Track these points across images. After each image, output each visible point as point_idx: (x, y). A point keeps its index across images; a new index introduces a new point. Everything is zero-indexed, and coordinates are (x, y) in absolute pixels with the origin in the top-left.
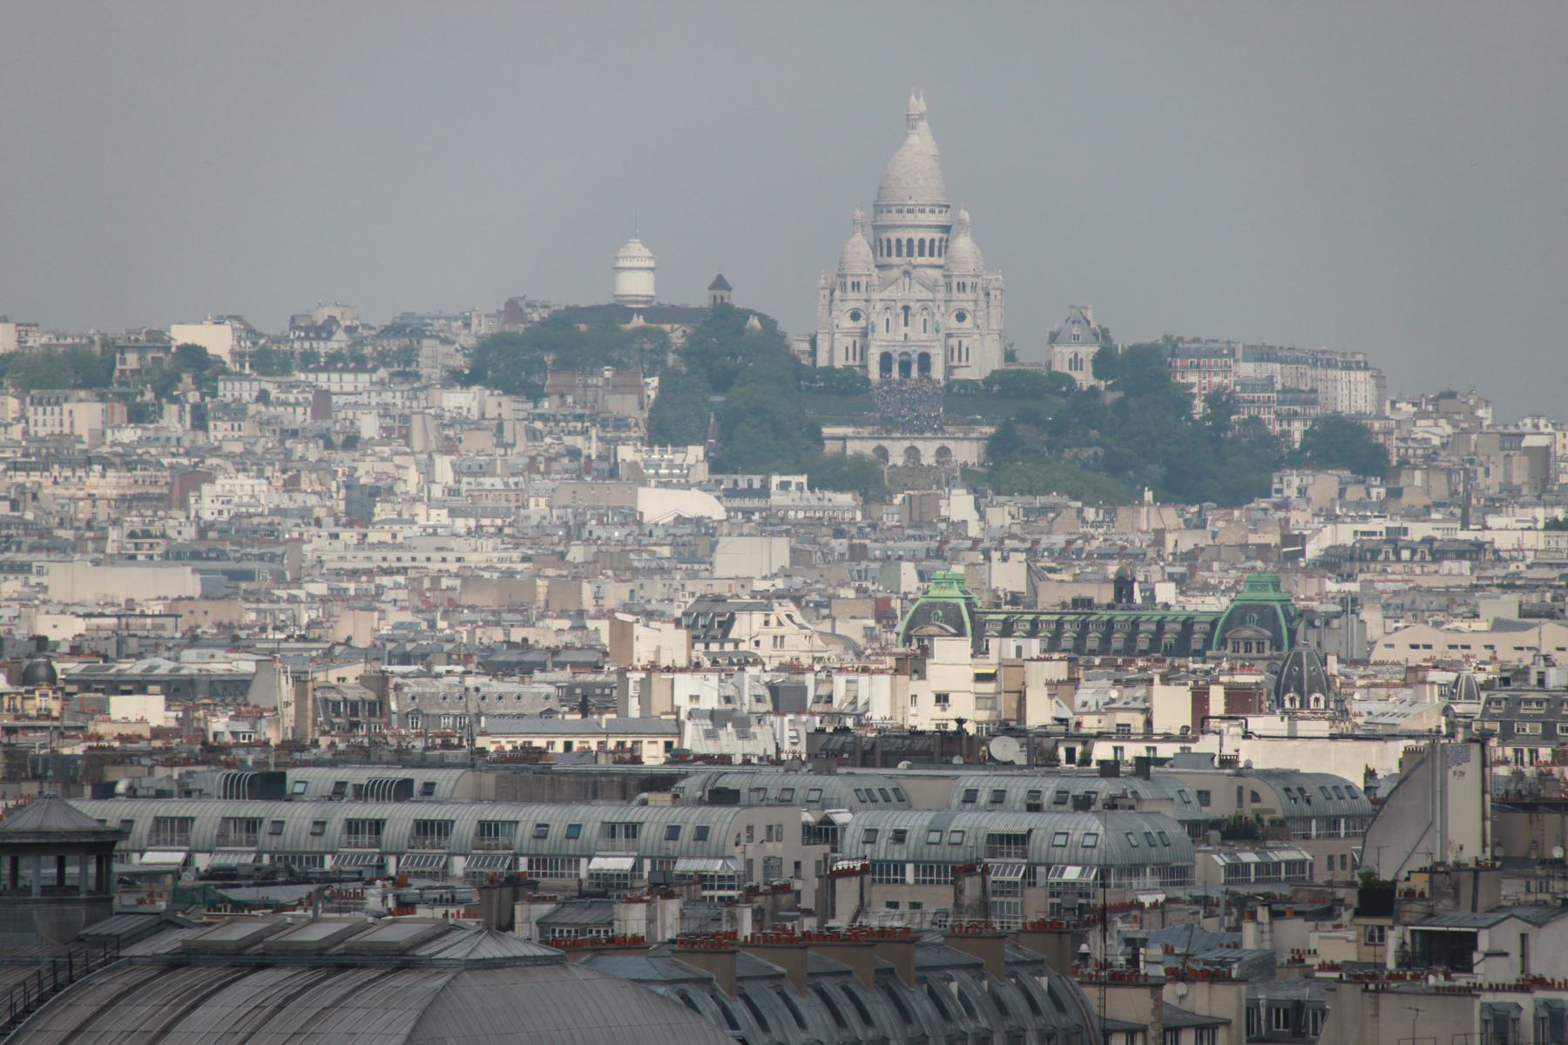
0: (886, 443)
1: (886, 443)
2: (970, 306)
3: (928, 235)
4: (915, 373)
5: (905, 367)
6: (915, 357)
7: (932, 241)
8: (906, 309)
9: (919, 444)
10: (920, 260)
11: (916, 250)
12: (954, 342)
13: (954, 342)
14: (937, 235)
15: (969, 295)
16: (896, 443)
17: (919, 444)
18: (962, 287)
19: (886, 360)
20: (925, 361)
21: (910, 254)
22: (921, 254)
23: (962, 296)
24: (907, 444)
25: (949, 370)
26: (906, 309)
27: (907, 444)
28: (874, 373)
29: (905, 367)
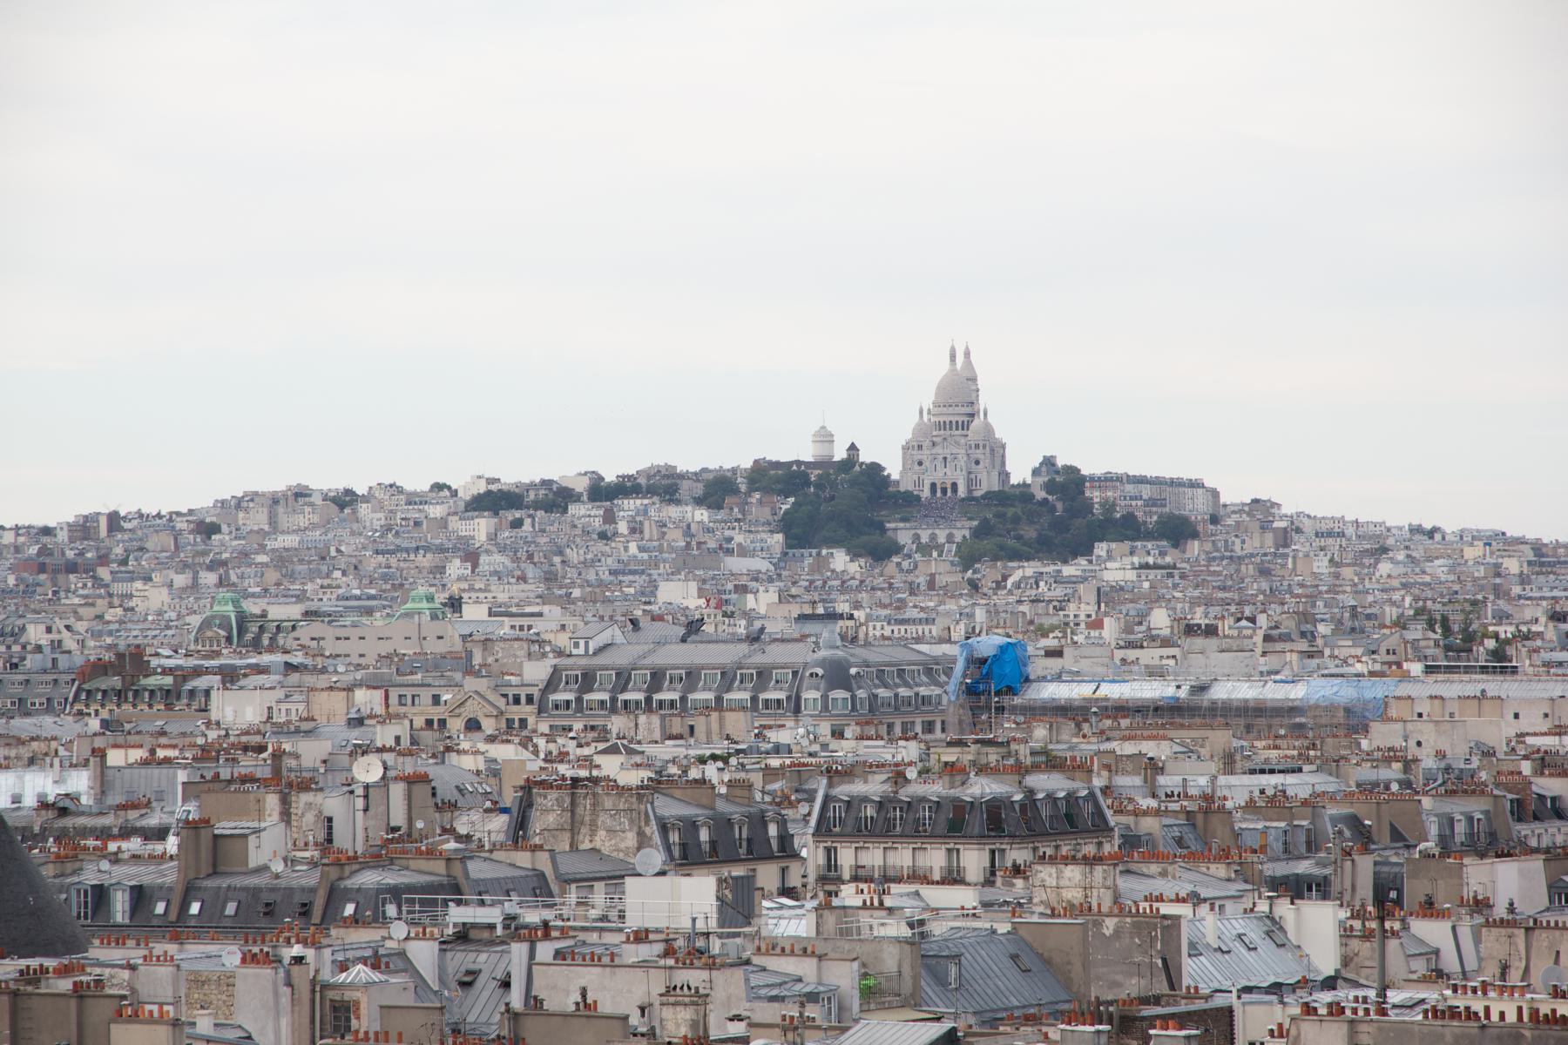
0: (919, 532)
1: (919, 532)
2: (981, 457)
3: (960, 419)
4: (949, 494)
5: (944, 491)
6: (949, 486)
7: (963, 422)
8: (945, 459)
9: (937, 531)
10: (957, 433)
11: (954, 427)
12: (973, 476)
13: (973, 476)
14: (966, 419)
15: (981, 450)
16: (924, 532)
17: (937, 531)
18: (977, 446)
19: (933, 486)
20: (954, 486)
21: (951, 429)
22: (957, 429)
23: (978, 451)
24: (931, 531)
25: (970, 491)
26: (945, 459)
27: (931, 531)
28: (926, 493)
29: (944, 491)
